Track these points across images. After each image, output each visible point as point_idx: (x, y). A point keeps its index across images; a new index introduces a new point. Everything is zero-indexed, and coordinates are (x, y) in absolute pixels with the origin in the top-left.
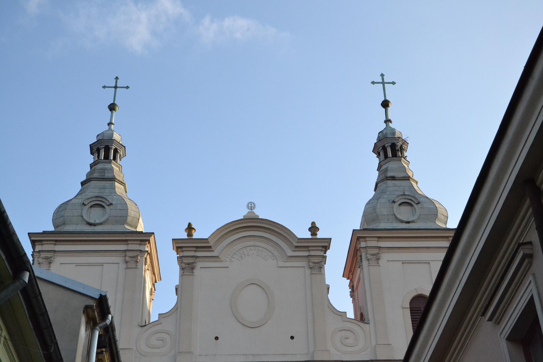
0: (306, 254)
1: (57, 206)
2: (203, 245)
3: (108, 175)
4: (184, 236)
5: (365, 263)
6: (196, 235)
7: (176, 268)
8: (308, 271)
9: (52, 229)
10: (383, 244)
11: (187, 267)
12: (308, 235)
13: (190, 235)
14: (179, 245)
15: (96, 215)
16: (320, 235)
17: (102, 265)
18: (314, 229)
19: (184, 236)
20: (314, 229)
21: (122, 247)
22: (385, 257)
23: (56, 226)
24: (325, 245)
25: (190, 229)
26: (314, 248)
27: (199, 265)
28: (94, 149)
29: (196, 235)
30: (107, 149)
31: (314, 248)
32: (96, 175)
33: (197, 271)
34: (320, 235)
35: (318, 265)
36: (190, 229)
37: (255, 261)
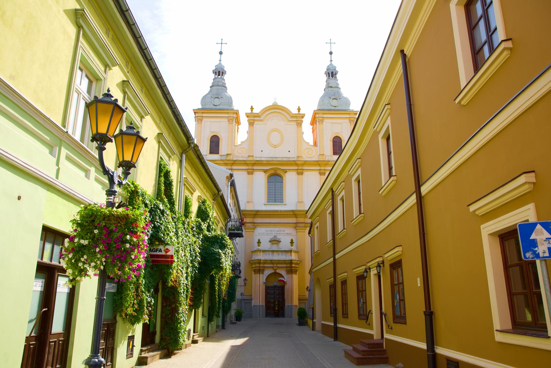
0: (295, 119)
1: (202, 97)
2: (257, 115)
3: (220, 84)
4: (250, 111)
5: (317, 123)
6: (254, 111)
7: (247, 124)
8: (296, 126)
9: (200, 107)
10: (324, 116)
11: (251, 124)
12: (297, 112)
13: (252, 111)
14: (248, 115)
15: (217, 102)
16: (301, 112)
17: (220, 122)
18: (299, 109)
19: (250, 111)
20: (299, 109)
21: (227, 115)
22: (326, 121)
23: (202, 106)
24: (303, 116)
25: (252, 108)
26: (298, 118)
27: (256, 123)
28: (215, 72)
29: (254, 111)
30: (219, 72)
31: (298, 118)
32: (216, 83)
33: (255, 125)
34: (301, 112)
35: (299, 124)
36: (252, 108)
37: (275, 122)
